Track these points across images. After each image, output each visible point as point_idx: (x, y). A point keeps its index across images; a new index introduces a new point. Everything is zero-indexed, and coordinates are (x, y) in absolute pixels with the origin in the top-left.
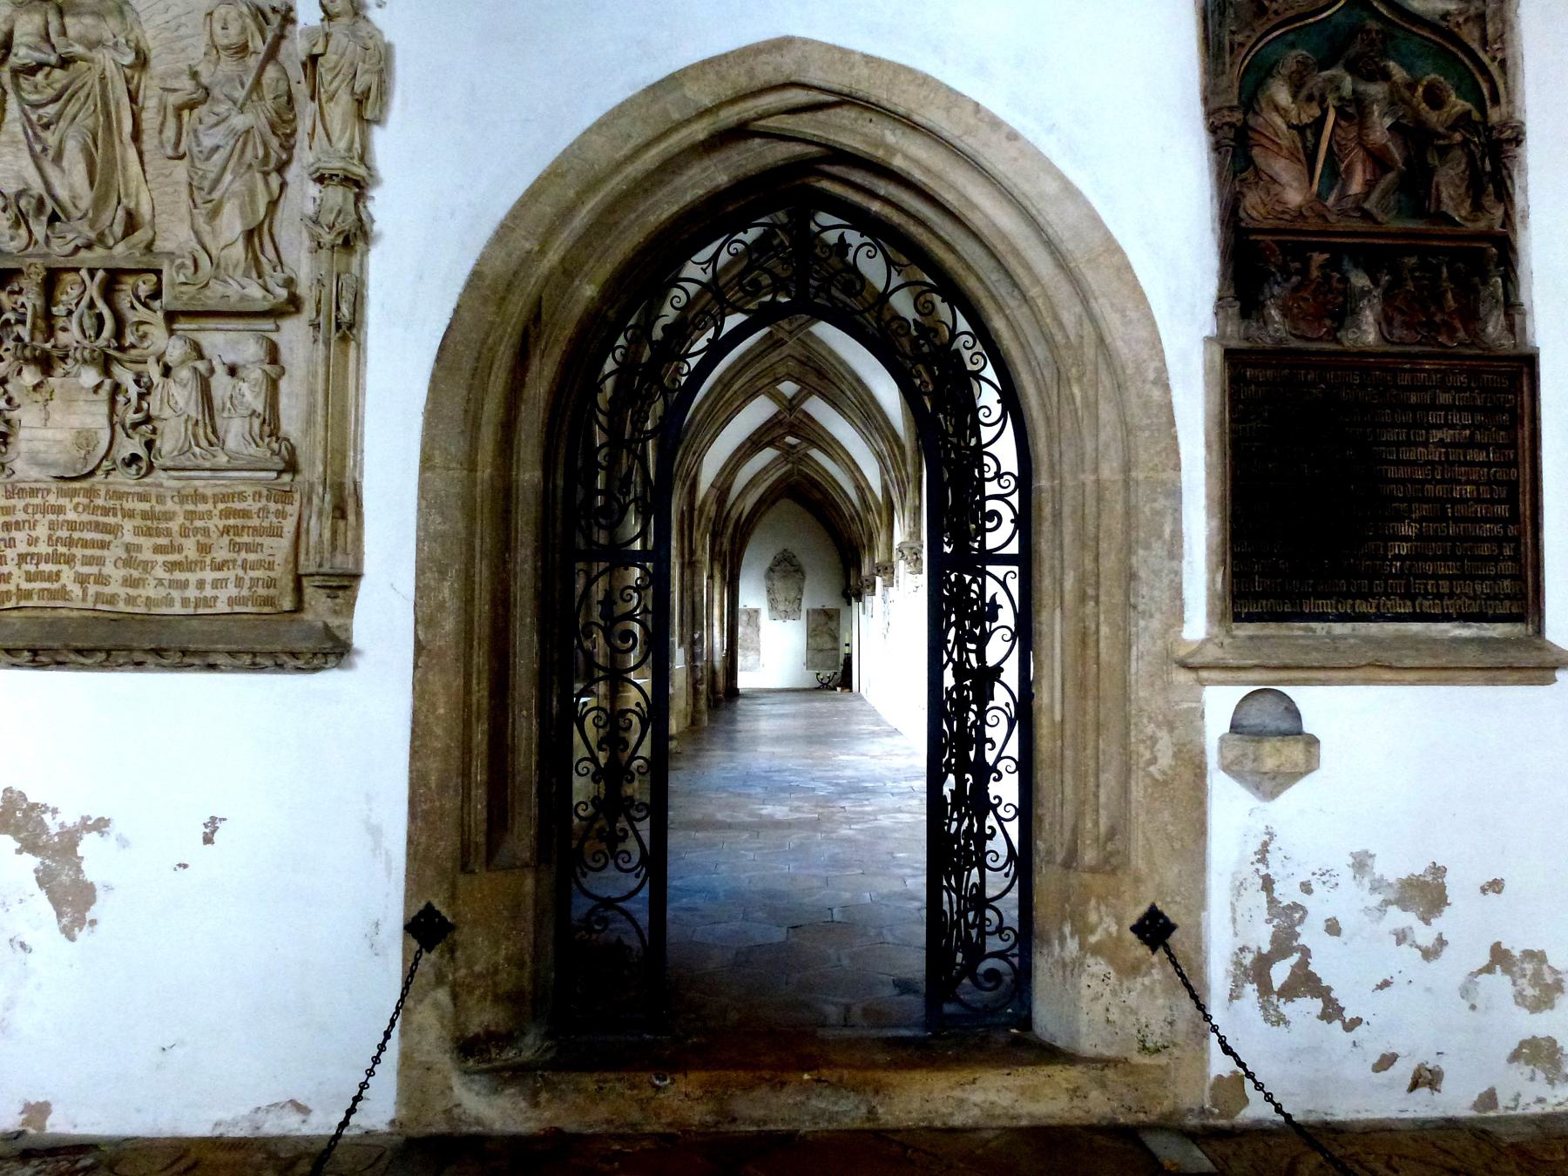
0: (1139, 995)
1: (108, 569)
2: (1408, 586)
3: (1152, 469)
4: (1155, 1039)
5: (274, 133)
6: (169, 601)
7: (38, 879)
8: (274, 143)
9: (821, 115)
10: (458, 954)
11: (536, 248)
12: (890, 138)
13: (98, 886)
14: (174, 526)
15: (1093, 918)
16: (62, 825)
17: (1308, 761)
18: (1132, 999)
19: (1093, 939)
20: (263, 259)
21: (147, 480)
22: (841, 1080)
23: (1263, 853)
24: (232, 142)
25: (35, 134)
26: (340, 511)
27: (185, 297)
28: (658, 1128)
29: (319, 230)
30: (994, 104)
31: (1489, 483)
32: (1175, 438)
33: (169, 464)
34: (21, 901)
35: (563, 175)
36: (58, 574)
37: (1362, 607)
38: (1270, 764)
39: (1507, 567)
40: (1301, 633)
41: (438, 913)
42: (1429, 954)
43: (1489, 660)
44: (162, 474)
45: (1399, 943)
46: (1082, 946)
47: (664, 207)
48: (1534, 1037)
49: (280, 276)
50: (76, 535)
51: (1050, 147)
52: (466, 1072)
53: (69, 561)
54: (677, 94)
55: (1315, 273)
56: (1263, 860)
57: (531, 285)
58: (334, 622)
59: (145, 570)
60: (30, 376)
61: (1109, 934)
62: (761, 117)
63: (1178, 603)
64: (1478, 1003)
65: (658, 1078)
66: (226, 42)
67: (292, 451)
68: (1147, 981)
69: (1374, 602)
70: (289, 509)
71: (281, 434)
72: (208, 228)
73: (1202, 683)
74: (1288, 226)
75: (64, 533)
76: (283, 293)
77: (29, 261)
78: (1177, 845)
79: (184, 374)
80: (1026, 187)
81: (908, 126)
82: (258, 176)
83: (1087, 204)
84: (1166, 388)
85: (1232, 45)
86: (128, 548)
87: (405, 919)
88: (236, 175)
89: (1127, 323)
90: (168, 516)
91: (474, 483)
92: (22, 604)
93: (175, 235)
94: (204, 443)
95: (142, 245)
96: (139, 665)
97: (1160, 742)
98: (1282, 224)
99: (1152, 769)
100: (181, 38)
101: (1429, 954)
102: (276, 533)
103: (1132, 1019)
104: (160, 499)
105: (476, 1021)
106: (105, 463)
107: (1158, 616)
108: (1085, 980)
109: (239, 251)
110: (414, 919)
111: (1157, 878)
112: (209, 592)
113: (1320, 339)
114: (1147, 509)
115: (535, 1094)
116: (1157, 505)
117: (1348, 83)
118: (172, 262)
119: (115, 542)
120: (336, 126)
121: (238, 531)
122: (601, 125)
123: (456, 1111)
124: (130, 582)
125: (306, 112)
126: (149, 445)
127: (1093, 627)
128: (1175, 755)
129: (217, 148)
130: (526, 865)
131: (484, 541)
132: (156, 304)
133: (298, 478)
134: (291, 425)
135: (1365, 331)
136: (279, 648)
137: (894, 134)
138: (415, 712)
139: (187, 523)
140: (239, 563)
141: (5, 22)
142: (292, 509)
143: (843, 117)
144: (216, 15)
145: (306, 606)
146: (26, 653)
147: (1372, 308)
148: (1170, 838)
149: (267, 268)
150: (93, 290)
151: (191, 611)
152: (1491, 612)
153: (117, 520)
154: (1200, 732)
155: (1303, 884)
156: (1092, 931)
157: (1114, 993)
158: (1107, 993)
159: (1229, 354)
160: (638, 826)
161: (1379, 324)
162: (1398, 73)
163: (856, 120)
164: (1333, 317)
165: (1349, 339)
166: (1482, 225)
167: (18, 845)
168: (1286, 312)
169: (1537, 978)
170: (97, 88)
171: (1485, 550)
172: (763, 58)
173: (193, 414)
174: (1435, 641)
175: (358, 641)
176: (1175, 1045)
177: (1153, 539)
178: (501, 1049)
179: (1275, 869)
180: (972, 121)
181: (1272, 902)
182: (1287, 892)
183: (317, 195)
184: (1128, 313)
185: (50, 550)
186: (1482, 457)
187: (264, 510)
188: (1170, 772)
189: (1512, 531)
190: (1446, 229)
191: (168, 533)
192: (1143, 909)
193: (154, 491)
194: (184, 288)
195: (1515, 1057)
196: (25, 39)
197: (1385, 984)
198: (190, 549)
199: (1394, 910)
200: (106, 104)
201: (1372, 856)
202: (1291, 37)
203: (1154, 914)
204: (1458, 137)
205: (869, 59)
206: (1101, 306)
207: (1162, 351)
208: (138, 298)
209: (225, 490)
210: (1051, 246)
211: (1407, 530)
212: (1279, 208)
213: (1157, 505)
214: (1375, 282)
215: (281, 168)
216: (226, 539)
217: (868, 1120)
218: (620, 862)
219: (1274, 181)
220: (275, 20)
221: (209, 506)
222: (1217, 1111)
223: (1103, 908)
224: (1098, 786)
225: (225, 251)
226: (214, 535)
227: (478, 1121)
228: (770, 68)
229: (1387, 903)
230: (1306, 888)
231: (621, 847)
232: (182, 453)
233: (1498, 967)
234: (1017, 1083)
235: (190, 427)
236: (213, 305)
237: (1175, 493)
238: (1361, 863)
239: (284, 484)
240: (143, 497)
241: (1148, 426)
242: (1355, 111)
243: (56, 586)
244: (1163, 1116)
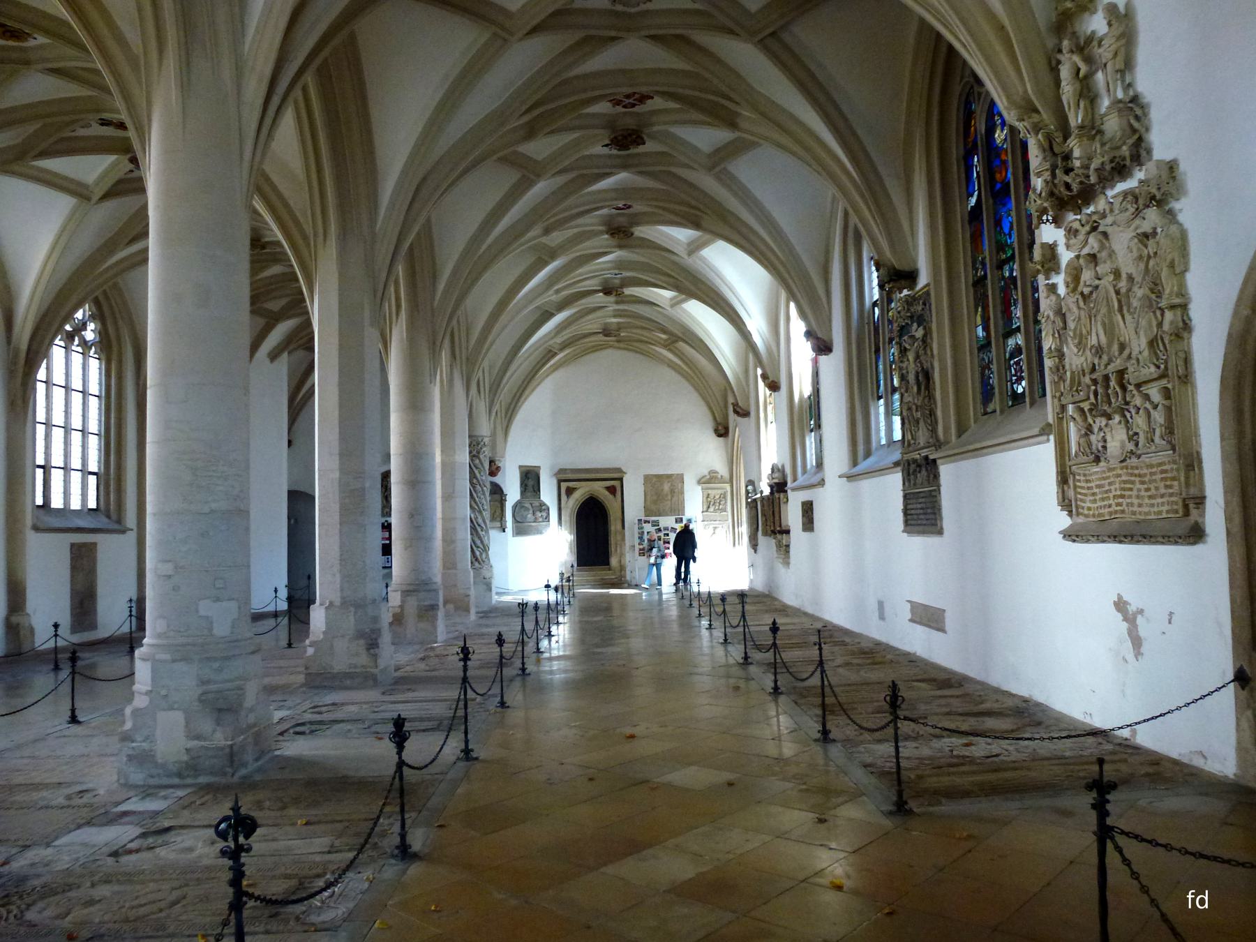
187: (1172, 469)
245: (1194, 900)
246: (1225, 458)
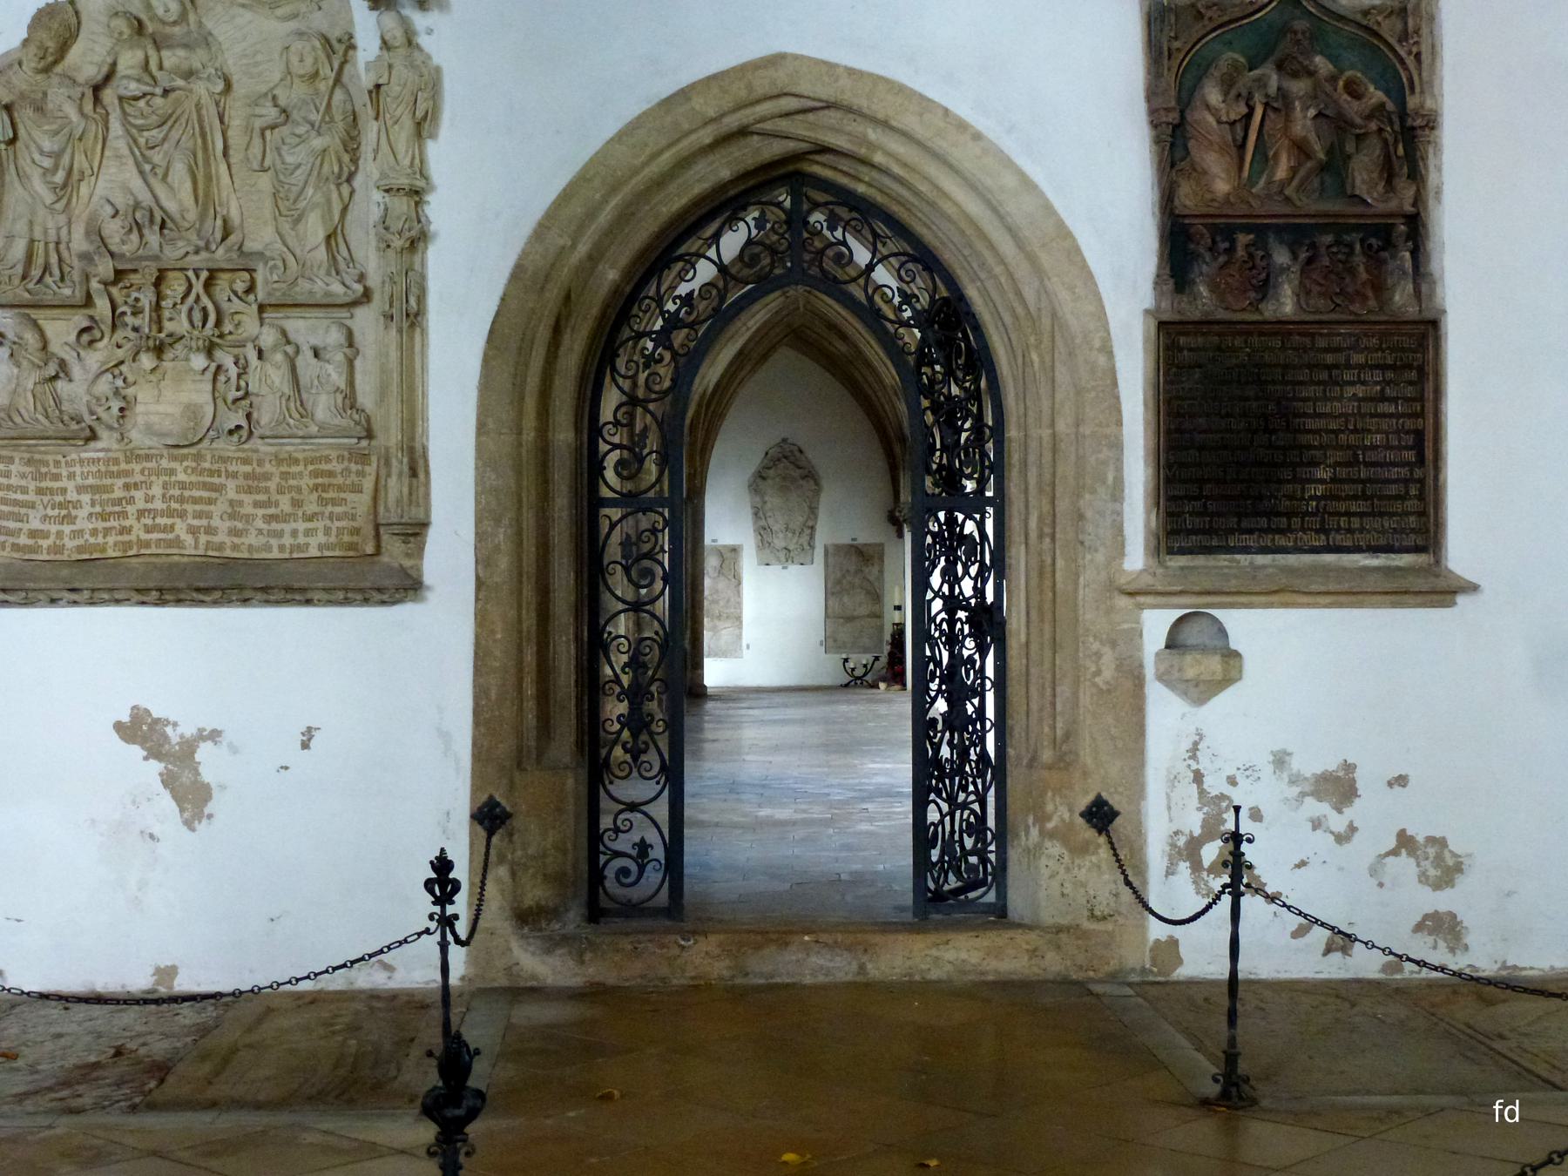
0: (1089, 870)
1: (216, 522)
2: (1323, 521)
3: (1097, 425)
5: (346, 151)
6: (269, 548)
7: (162, 782)
8: (346, 158)
9: (811, 117)
10: (516, 837)
11: (570, 243)
13: (213, 786)
14: (272, 485)
15: (1050, 807)
16: (182, 736)
17: (1226, 671)
18: (1082, 874)
19: (1050, 825)
20: (339, 258)
21: (246, 446)
22: (836, 942)
23: (1194, 751)
24: (311, 160)
25: (142, 154)
26: (414, 473)
27: (278, 294)
28: (684, 982)
29: (389, 236)
30: (962, 109)
31: (1397, 432)
32: (1118, 398)
33: (268, 433)
34: (149, 800)
35: (589, 180)
36: (172, 527)
37: (1281, 541)
38: (1190, 673)
39: (1411, 505)
40: (1226, 563)
41: (498, 804)
42: (1341, 839)
43: (1388, 586)
44: (260, 441)
45: (1314, 829)
46: (1042, 832)
47: (674, 201)
48: (1436, 912)
49: (354, 272)
50: (187, 493)
51: (1010, 146)
52: (523, 937)
53: (182, 515)
55: (1240, 252)
56: (1194, 757)
57: (565, 273)
58: (407, 563)
59: (247, 522)
60: (147, 361)
61: (1063, 821)
64: (1386, 881)
65: (683, 939)
66: (302, 72)
67: (368, 420)
68: (1094, 859)
69: (1292, 536)
70: (367, 469)
71: (358, 405)
72: (293, 233)
73: (1141, 607)
74: (1217, 212)
75: (177, 492)
76: (359, 288)
77: (144, 263)
78: (1120, 744)
79: (279, 357)
80: (989, 182)
82: (333, 187)
83: (1041, 195)
84: (1110, 354)
85: (1169, 49)
86: (232, 503)
87: (471, 809)
88: (317, 188)
90: (267, 477)
91: (520, 445)
92: (143, 551)
93: (261, 236)
94: (297, 416)
95: (236, 248)
96: (245, 602)
97: (1105, 657)
98: (1212, 211)
99: (1097, 679)
100: (257, 64)
101: (1341, 839)
102: (357, 489)
103: (1082, 891)
104: (260, 463)
105: (530, 895)
106: (211, 433)
107: (1102, 549)
108: (1044, 861)
109: (322, 254)
110: (480, 809)
111: (1102, 771)
112: (301, 540)
113: (1244, 310)
115: (581, 954)
116: (1101, 456)
117: (1274, 81)
118: (266, 263)
119: (221, 499)
120: (401, 147)
121: (325, 488)
122: (620, 137)
123: (515, 969)
124: (234, 532)
125: (370, 132)
126: (249, 416)
127: (1049, 561)
128: (1119, 668)
129: (299, 165)
130: (566, 768)
131: (530, 496)
132: (251, 297)
133: (374, 443)
134: (366, 397)
135: (1283, 303)
136: (368, 584)
138: (477, 637)
139: (283, 483)
140: (327, 514)
141: (109, 53)
142: (371, 470)
144: (292, 49)
145: (383, 550)
146: (154, 593)
147: (1290, 282)
148: (1113, 738)
149: (342, 265)
150: (198, 287)
151: (287, 556)
152: (1397, 544)
153: (222, 480)
154: (1140, 648)
155: (1228, 778)
156: (1049, 818)
157: (1068, 870)
158: (1062, 871)
159: (1161, 325)
161: (1298, 295)
162: (1321, 63)
163: (842, 119)
164: (1256, 289)
165: (1269, 311)
166: (1393, 205)
167: (145, 753)
168: (1214, 287)
169: (1439, 861)
170: (195, 116)
171: (1393, 489)
172: (761, 73)
173: (286, 391)
174: (1345, 569)
175: (428, 579)
176: (1120, 914)
178: (549, 921)
179: (1204, 764)
180: (942, 124)
181: (1202, 793)
182: (1214, 785)
183: (381, 200)
185: (164, 506)
186: (1392, 409)
187: (347, 469)
189: (1418, 473)
190: (1359, 209)
191: (267, 490)
192: (1090, 798)
193: (255, 456)
194: (275, 286)
195: (1419, 928)
196: (129, 72)
197: (1302, 864)
198: (285, 504)
199: (1309, 800)
200: (202, 128)
201: (1290, 754)
202: (1228, 36)
204: (1373, 126)
205: (851, 72)
206: (1055, 284)
208: (235, 293)
209: (314, 454)
210: (1011, 231)
211: (1322, 473)
212: (1208, 196)
213: (1101, 456)
214: (1295, 257)
215: (349, 180)
216: (315, 495)
217: (859, 973)
219: (1205, 173)
220: (340, 48)
221: (300, 468)
222: (1155, 970)
223: (1058, 799)
224: (1054, 696)
225: (313, 253)
226: (305, 491)
227: (533, 977)
229: (1303, 794)
230: (1232, 781)
231: (643, 758)
232: (279, 423)
233: (1403, 850)
234: (986, 944)
235: (284, 402)
236: (301, 299)
237: (1117, 445)
238: (1280, 760)
239: (364, 448)
240: (246, 461)
241: (1094, 388)
242: (1280, 105)
243: (171, 536)
245: (1501, 1111)
246: (484, 459)
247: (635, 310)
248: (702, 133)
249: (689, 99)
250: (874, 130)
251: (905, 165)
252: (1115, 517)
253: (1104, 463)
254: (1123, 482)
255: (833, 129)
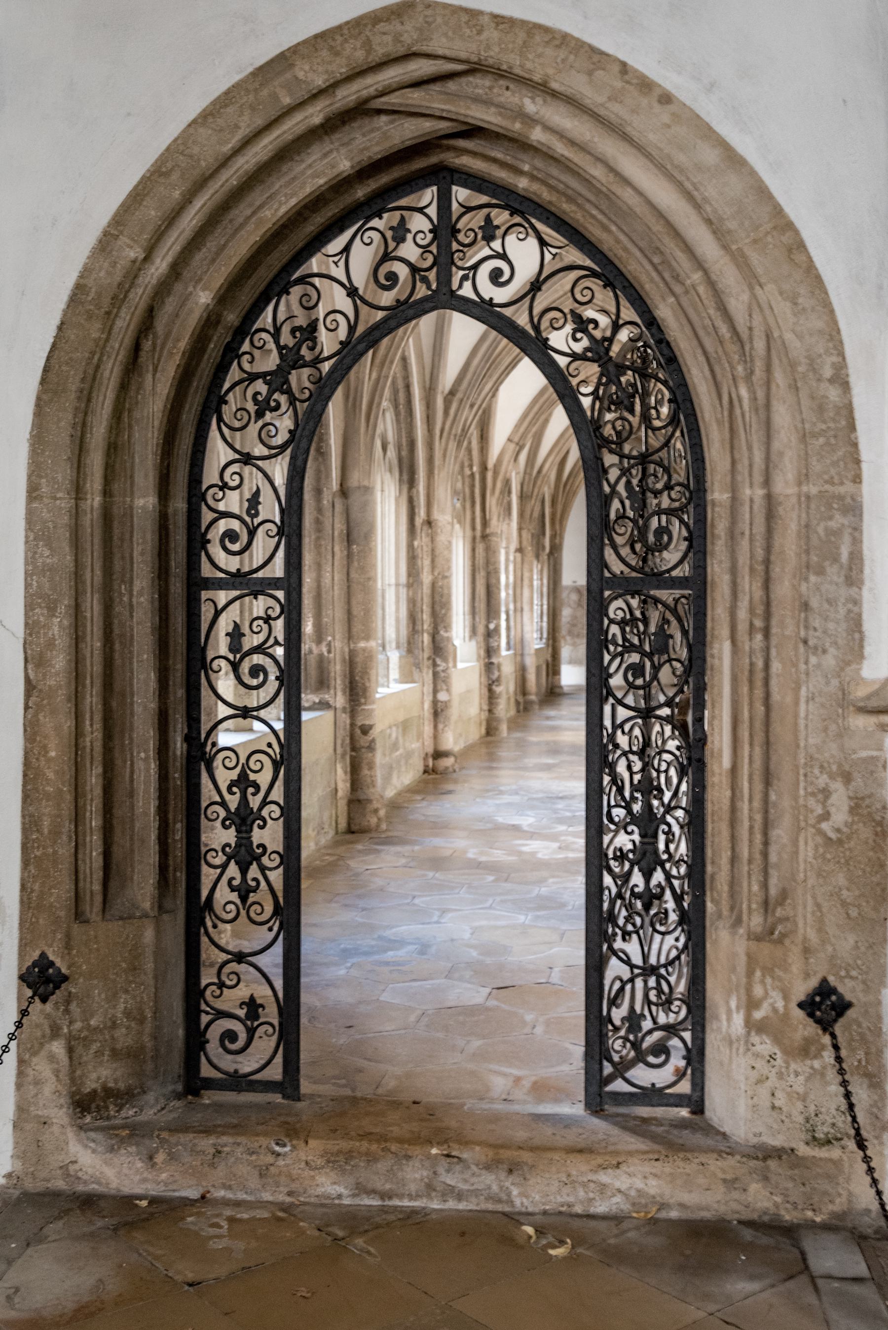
0: (808, 1079)
3: (826, 482)
4: (826, 1130)
12: (530, 107)
15: (758, 991)
19: (758, 1015)
32: (855, 445)
46: (749, 1023)
54: (288, 75)
61: (775, 1010)
62: (382, 94)
63: (857, 636)
68: (817, 1064)
78: (854, 913)
80: (681, 158)
81: (548, 93)
83: (753, 173)
84: (845, 386)
89: (799, 311)
99: (824, 826)
107: (832, 651)
111: (830, 949)
114: (821, 530)
116: (832, 524)
127: (760, 664)
128: (853, 810)
137: (534, 102)
143: (477, 86)
148: (844, 904)
157: (780, 1076)
158: (773, 1076)
160: (272, 875)
163: (491, 88)
172: (382, 27)
177: (827, 563)
180: (618, 84)
184: (800, 300)
188: (845, 830)
192: (813, 983)
203: (825, 990)
207: (841, 342)
218: (252, 915)
223: (769, 980)
224: (766, 843)
228: (388, 39)
241: (822, 433)
244: (834, 1215)
247: (246, 347)
248: (310, 110)
249: (292, 66)
250: (532, 98)
251: (572, 143)
252: (850, 606)
253: (837, 533)
254: (861, 560)
255: (477, 100)
